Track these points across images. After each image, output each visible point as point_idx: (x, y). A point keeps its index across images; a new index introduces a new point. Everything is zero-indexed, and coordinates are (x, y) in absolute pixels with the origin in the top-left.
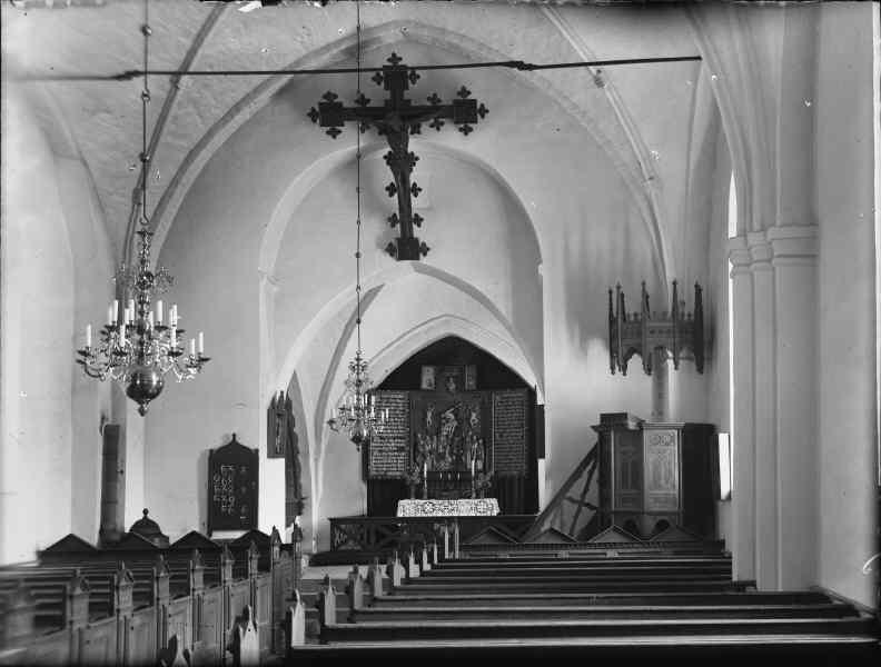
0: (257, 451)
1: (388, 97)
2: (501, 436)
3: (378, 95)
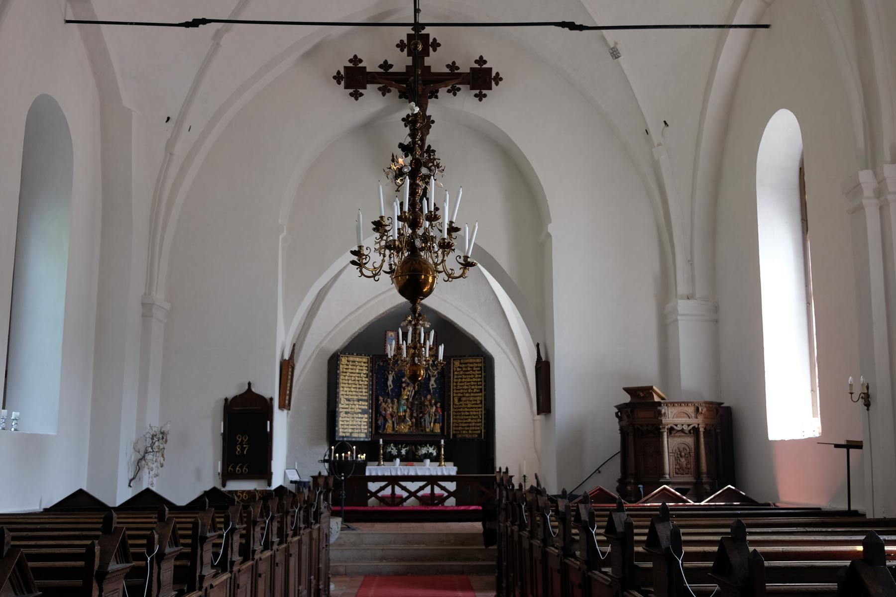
1: (411, 64)
2: (459, 400)
3: (400, 61)
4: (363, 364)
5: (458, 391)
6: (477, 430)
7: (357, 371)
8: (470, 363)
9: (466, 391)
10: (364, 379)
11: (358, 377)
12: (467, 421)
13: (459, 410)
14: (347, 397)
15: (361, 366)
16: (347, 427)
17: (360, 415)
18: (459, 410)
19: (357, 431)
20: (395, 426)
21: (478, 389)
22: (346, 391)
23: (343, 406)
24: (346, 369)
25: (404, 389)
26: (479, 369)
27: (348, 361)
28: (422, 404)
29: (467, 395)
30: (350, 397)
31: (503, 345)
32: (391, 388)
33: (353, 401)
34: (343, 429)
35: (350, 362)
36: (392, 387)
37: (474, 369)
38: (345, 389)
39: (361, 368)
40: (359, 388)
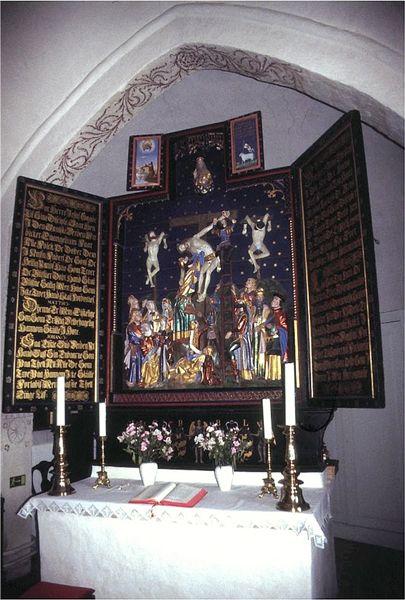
7: (71, 231)
11: (72, 247)
16: (40, 375)
17: (74, 344)
22: (39, 279)
23: (26, 318)
24: (40, 221)
27: (46, 203)
30: (49, 295)
32: (155, 272)
34: (27, 380)
36: (158, 269)
39: (81, 226)
40: (75, 275)
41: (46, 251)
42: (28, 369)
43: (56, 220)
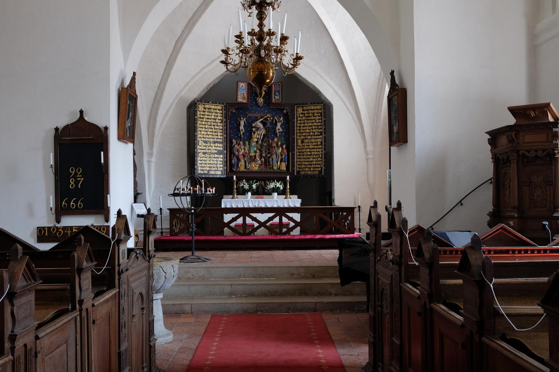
0: (106, 128)
2: (302, 142)
4: (218, 111)
5: (301, 134)
6: (318, 168)
7: (213, 117)
8: (312, 110)
9: (308, 134)
10: (219, 124)
11: (214, 122)
12: (309, 160)
13: (302, 150)
14: (204, 139)
15: (216, 113)
16: (205, 165)
17: (216, 156)
18: (302, 150)
19: (214, 169)
20: (247, 165)
21: (318, 132)
22: (203, 135)
23: (200, 148)
24: (203, 115)
25: (254, 133)
26: (319, 114)
27: (204, 108)
28: (270, 146)
29: (309, 137)
30: (207, 140)
31: (340, 93)
32: (243, 132)
33: (210, 143)
34: (201, 167)
35: (207, 109)
37: (315, 115)
38: (203, 133)
39: (216, 115)
40: (215, 132)
41: (205, 125)
42: (201, 164)
43: (208, 114)
